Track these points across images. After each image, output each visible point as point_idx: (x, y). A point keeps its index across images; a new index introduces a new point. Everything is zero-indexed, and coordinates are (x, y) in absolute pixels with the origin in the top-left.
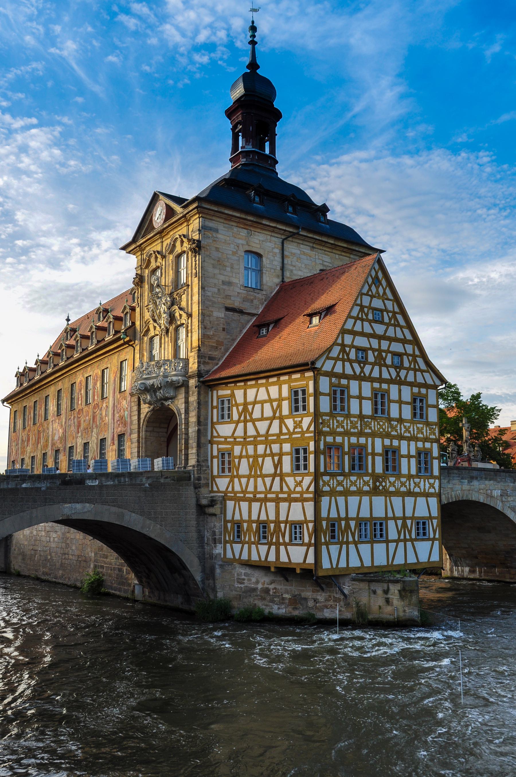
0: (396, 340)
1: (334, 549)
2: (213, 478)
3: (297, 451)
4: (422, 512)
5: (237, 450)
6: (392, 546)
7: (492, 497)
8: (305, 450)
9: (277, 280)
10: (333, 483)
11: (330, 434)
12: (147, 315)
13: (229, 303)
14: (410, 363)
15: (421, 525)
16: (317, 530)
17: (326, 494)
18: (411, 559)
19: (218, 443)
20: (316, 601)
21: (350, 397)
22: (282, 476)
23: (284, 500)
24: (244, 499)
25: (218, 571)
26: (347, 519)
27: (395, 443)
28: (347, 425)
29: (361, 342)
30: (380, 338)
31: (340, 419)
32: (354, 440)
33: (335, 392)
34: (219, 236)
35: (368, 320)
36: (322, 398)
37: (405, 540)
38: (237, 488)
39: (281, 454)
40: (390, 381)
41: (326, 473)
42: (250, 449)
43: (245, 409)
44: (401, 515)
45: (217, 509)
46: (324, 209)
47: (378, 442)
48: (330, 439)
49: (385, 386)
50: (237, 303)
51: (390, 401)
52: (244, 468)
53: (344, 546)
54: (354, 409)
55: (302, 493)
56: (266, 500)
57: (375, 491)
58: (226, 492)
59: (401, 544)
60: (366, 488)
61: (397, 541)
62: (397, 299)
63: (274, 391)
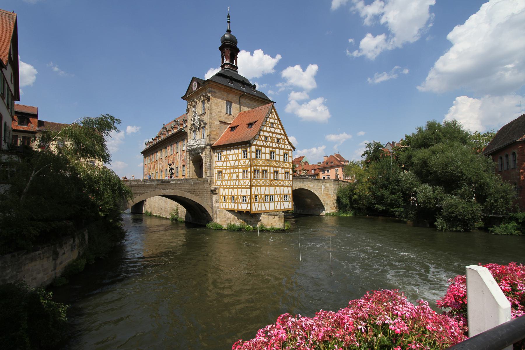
1: (257, 204)
2: (216, 181)
3: (244, 172)
4: (286, 192)
5: (224, 171)
6: (276, 203)
8: (247, 171)
9: (238, 112)
10: (256, 182)
12: (192, 123)
15: (286, 196)
16: (250, 198)
17: (253, 186)
18: (282, 208)
19: (217, 169)
20: (251, 221)
22: (239, 180)
23: (240, 188)
24: (226, 188)
25: (218, 212)
26: (261, 195)
27: (277, 169)
28: (261, 163)
29: (266, 134)
30: (273, 133)
32: (263, 168)
33: (257, 151)
35: (268, 126)
37: (280, 202)
38: (224, 184)
39: (239, 173)
40: (276, 148)
41: (253, 179)
42: (228, 171)
43: (226, 157)
45: (217, 192)
46: (254, 86)
47: (272, 168)
48: (255, 167)
49: (274, 150)
50: (223, 120)
52: (226, 177)
54: (264, 158)
55: (246, 186)
56: (234, 188)
57: (271, 185)
58: (220, 186)
59: (279, 203)
62: (279, 120)
63: (236, 151)
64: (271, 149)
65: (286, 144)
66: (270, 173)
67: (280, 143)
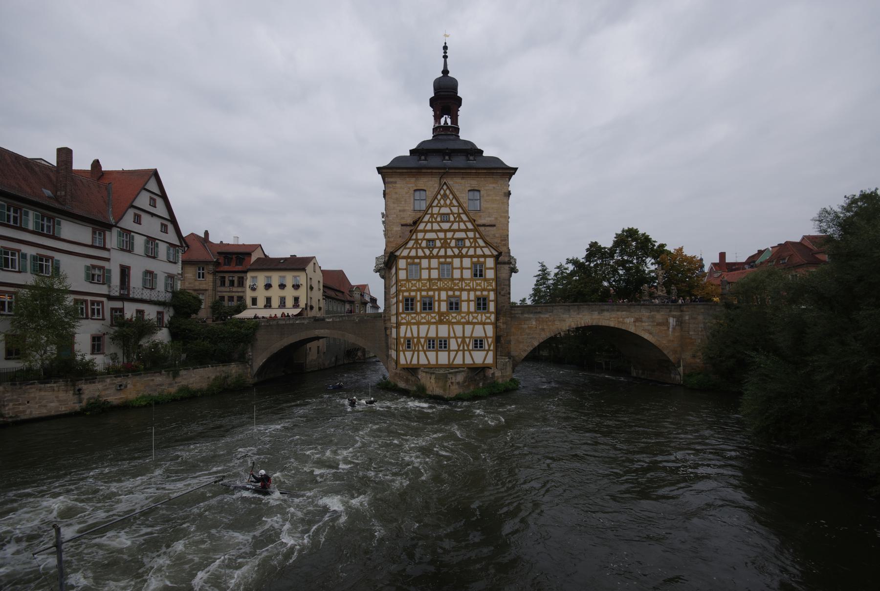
0: (460, 230)
1: (409, 354)
6: (453, 354)
7: (623, 323)
10: (408, 318)
11: (406, 291)
13: (403, 222)
14: (471, 243)
18: (468, 361)
21: (421, 269)
26: (418, 338)
27: (457, 293)
28: (419, 285)
31: (414, 282)
32: (424, 293)
34: (397, 185)
35: (436, 222)
36: (400, 272)
37: (464, 350)
40: (455, 256)
44: (461, 335)
48: (406, 294)
49: (449, 260)
51: (453, 268)
53: (416, 353)
57: (441, 322)
59: (460, 353)
60: (433, 320)
61: (457, 351)
62: (460, 205)
64: (442, 260)
65: (479, 247)
66: (439, 301)
67: (464, 247)
